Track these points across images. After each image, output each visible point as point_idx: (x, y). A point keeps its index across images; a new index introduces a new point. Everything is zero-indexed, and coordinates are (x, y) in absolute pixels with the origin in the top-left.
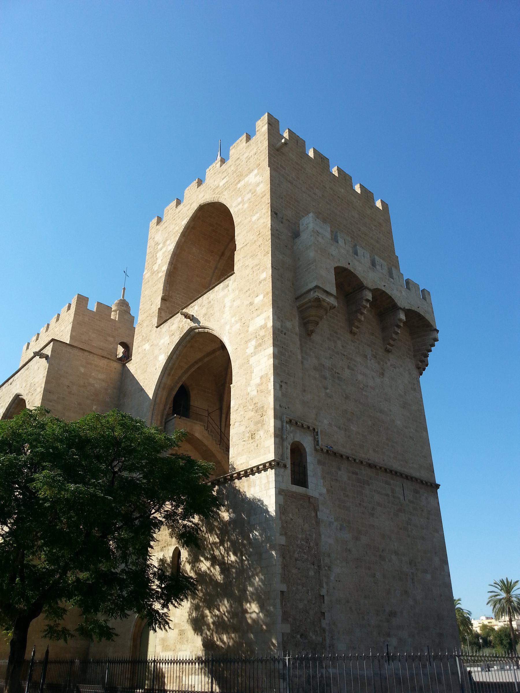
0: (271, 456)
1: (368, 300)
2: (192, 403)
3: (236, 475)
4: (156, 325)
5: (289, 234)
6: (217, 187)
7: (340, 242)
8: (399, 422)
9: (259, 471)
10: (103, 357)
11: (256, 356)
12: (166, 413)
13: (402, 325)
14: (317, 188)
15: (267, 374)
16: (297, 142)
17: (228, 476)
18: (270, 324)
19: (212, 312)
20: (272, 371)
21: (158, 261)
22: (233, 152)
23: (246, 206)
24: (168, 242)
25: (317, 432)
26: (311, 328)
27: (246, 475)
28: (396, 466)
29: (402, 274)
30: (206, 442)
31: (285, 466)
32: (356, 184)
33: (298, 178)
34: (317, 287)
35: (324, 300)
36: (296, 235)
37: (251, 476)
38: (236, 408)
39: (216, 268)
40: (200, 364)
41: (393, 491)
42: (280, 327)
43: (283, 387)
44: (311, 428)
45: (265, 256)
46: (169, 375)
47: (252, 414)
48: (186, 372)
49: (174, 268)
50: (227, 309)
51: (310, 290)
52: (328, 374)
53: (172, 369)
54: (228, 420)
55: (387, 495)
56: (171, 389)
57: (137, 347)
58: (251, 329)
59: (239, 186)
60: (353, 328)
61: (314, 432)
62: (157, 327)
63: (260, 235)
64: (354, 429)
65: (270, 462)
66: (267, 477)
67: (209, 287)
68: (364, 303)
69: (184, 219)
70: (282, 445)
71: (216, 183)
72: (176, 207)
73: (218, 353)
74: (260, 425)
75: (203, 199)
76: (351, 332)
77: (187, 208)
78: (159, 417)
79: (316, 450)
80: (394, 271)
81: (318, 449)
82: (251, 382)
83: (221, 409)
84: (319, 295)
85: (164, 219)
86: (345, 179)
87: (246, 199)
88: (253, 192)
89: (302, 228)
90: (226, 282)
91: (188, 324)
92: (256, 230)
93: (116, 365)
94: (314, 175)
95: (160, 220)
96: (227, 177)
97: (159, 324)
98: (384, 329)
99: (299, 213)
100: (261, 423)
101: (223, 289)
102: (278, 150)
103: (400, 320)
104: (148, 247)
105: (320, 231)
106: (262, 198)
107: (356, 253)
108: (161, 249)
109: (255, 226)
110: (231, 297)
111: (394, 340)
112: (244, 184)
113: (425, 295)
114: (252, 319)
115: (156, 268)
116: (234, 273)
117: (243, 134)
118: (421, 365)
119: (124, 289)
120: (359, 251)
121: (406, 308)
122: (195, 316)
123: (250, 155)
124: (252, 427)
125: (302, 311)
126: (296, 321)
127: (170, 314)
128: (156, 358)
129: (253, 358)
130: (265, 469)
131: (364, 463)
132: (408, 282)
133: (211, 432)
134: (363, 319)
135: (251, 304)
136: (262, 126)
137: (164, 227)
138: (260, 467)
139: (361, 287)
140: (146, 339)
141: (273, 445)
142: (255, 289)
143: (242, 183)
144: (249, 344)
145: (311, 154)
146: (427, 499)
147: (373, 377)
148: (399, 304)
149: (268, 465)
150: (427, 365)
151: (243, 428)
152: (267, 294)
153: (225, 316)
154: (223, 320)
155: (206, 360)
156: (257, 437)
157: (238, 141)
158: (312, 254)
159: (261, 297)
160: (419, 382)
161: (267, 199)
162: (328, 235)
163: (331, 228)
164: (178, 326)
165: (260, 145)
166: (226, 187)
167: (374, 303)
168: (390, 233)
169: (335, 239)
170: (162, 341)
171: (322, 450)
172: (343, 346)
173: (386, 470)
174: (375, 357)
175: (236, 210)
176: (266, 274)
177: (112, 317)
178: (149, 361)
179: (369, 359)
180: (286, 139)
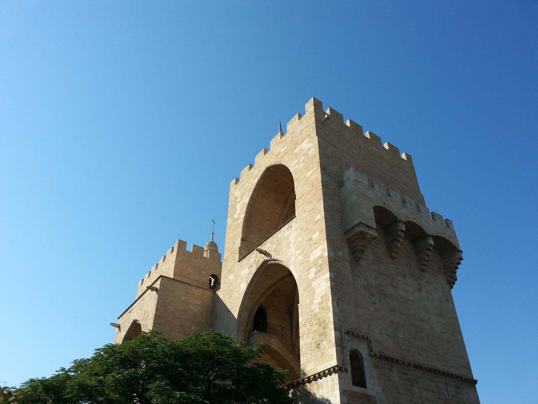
0: (334, 362)
1: (402, 231)
2: (268, 321)
3: (306, 379)
6: (279, 154)
8: (437, 329)
9: (325, 376)
10: (198, 287)
11: (317, 280)
12: (248, 329)
13: (432, 249)
16: (336, 116)
18: (326, 254)
20: (330, 292)
22: (290, 127)
23: (301, 166)
24: (244, 197)
26: (358, 255)
27: (315, 379)
28: (439, 366)
30: (281, 352)
31: (346, 370)
32: (385, 142)
35: (367, 233)
36: (341, 184)
38: (303, 323)
39: (282, 213)
40: (273, 289)
45: (318, 202)
46: (249, 298)
47: (317, 327)
48: (262, 296)
49: (250, 215)
50: (292, 245)
51: (355, 226)
53: (251, 293)
55: (434, 391)
58: (312, 259)
59: (295, 151)
61: (368, 340)
62: (239, 262)
65: (334, 368)
66: (332, 380)
67: (277, 228)
68: (400, 233)
70: (343, 353)
71: (278, 150)
73: (286, 279)
74: (323, 336)
78: (243, 333)
79: (371, 355)
80: (421, 207)
81: (373, 355)
83: (291, 324)
86: (376, 140)
88: (306, 155)
89: (345, 179)
91: (262, 258)
93: (209, 293)
95: (237, 181)
100: (324, 335)
101: (288, 229)
103: (430, 245)
105: (359, 180)
107: (389, 195)
109: (310, 180)
110: (294, 234)
111: (427, 261)
112: (299, 149)
113: (448, 223)
114: (312, 251)
118: (451, 280)
119: (213, 233)
121: (434, 235)
124: (317, 338)
125: (350, 242)
126: (346, 251)
128: (239, 285)
130: (330, 374)
131: (412, 365)
132: (433, 214)
134: (399, 246)
135: (310, 239)
136: (310, 107)
137: (241, 185)
139: (395, 220)
140: (231, 271)
142: (313, 228)
143: (297, 149)
145: (348, 124)
147: (412, 292)
149: (332, 369)
150: (456, 280)
151: (310, 340)
152: (322, 231)
153: (290, 250)
154: (289, 254)
155: (278, 285)
157: (293, 119)
158: (354, 198)
159: (317, 234)
161: (317, 159)
162: (366, 183)
163: (368, 177)
164: (255, 260)
165: (309, 120)
166: (286, 153)
168: (415, 177)
170: (243, 272)
171: (376, 355)
172: (385, 269)
173: (430, 370)
175: (294, 169)
176: (320, 216)
178: (234, 288)
180: (328, 115)
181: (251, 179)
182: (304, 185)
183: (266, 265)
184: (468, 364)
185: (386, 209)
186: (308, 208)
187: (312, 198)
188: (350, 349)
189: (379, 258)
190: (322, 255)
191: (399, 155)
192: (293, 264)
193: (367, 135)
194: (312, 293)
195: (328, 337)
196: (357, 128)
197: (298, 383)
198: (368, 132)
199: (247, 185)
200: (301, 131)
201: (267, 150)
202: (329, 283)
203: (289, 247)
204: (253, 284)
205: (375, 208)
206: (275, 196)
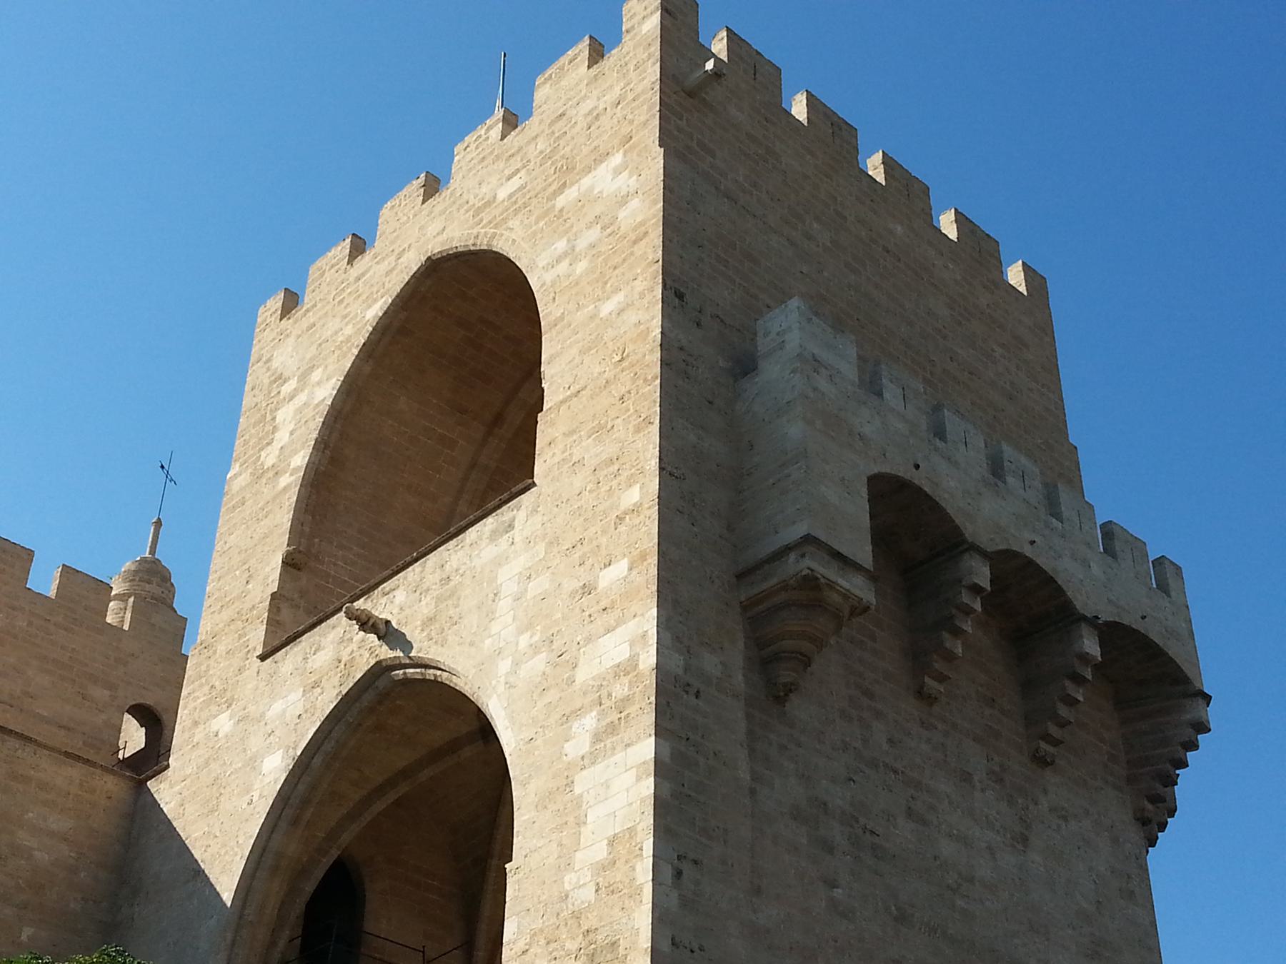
1: (976, 589)
2: (369, 925)
4: (259, 651)
6: (488, 204)
7: (886, 395)
10: (68, 755)
11: (599, 767)
18: (649, 659)
19: (451, 613)
22: (544, 93)
23: (581, 267)
24: (316, 375)
26: (785, 675)
29: (1091, 506)
34: (808, 539)
35: (831, 585)
36: (745, 366)
38: (521, 945)
39: (473, 466)
40: (404, 788)
42: (680, 672)
45: (638, 430)
46: (295, 822)
49: (332, 460)
50: (504, 604)
53: (305, 802)
57: (188, 723)
58: (584, 675)
62: (263, 658)
63: (625, 364)
67: (446, 526)
68: (966, 598)
69: (376, 301)
72: (350, 262)
73: (467, 752)
75: (440, 239)
76: (922, 694)
77: (384, 266)
80: (1064, 495)
84: (814, 565)
85: (308, 300)
86: (907, 191)
87: (582, 244)
88: (607, 223)
89: (763, 344)
90: (505, 514)
91: (367, 652)
93: (113, 786)
95: (291, 302)
96: (523, 173)
101: (494, 536)
102: (691, 94)
103: (1084, 658)
104: (247, 388)
106: (635, 242)
109: (611, 333)
110: (520, 563)
111: (1063, 724)
113: (1166, 575)
114: (589, 640)
115: (269, 457)
116: (534, 484)
118: (1154, 813)
119: (158, 524)
120: (948, 427)
121: (1104, 617)
122: (394, 624)
123: (601, 107)
126: (737, 653)
127: (309, 613)
128: (253, 763)
129: (585, 772)
132: (1109, 531)
134: (959, 650)
135: (587, 589)
137: (305, 323)
139: (953, 543)
140: (222, 699)
142: (603, 540)
143: (571, 193)
144: (576, 725)
148: (1078, 605)
150: (1172, 812)
152: (643, 557)
154: (488, 642)
157: (564, 60)
158: (795, 430)
159: (620, 568)
161: (652, 247)
162: (850, 371)
164: (336, 655)
165: (632, 75)
166: (518, 204)
167: (996, 599)
169: (872, 385)
170: (278, 706)
172: (890, 741)
174: (1000, 781)
175: (548, 277)
176: (641, 492)
177: (109, 620)
181: (350, 301)
182: (582, 352)
183: (381, 683)
185: (919, 490)
186: (591, 451)
187: (612, 413)
189: (869, 694)
190: (633, 662)
192: (501, 689)
194: (572, 818)
199: (333, 325)
200: (595, 117)
201: (437, 181)
203: (491, 616)
204: (317, 760)
205: (874, 481)
206: (450, 391)
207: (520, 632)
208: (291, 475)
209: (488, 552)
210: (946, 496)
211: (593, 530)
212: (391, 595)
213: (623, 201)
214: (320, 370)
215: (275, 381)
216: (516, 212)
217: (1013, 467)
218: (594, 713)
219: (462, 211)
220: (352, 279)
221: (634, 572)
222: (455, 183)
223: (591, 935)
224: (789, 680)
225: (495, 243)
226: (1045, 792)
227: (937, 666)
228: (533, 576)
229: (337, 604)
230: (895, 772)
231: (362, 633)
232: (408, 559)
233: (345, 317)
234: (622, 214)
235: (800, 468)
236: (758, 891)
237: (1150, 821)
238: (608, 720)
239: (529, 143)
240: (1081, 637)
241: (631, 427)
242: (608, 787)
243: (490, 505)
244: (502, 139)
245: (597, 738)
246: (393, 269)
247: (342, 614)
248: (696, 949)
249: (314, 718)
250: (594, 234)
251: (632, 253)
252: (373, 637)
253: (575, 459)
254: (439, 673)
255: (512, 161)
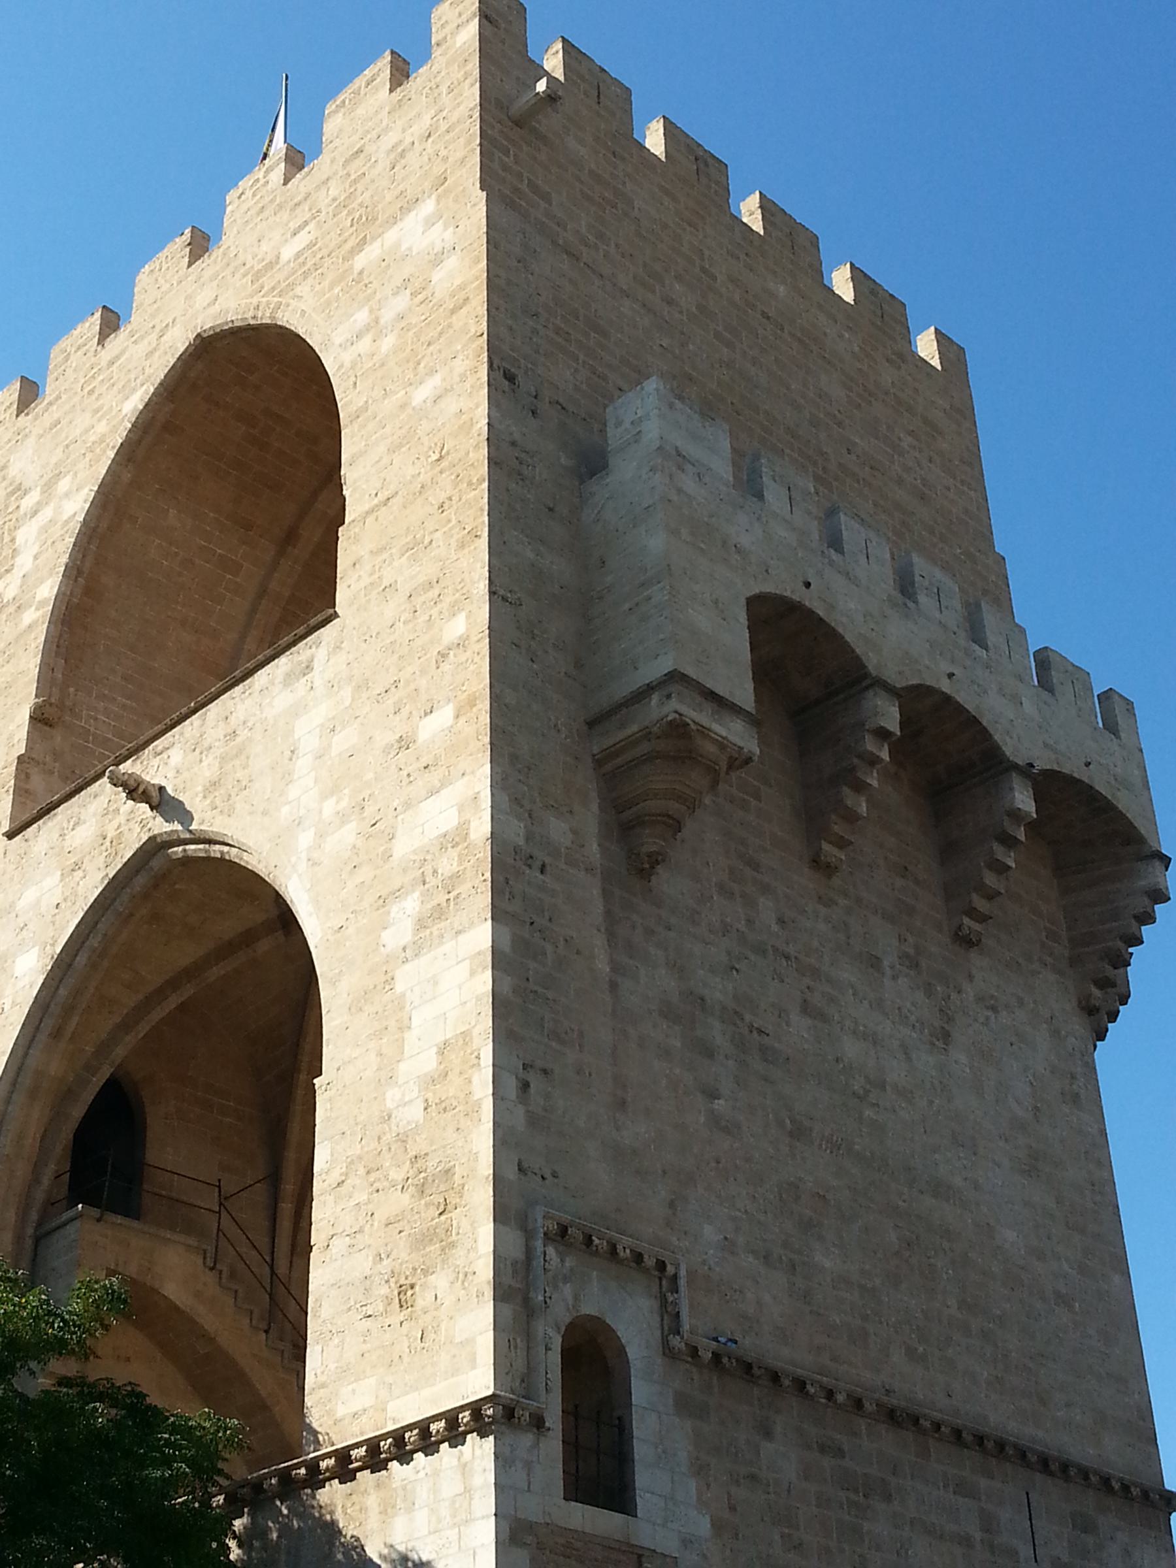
0: (478, 1381)
1: (883, 734)
2: (152, 1155)
4: (6, 827)
5: (563, 460)
6: (270, 265)
8: (1010, 1235)
9: (428, 1446)
11: (424, 960)
12: (40, 1195)
14: (678, 278)
15: (466, 1036)
16: (596, 92)
17: (297, 1466)
18: (481, 826)
19: (239, 775)
20: (487, 1022)
21: (19, 560)
23: (388, 343)
24: (64, 485)
25: (675, 1278)
26: (650, 842)
27: (376, 1459)
28: (1002, 1417)
29: (1022, 631)
30: (208, 1321)
31: (538, 1423)
33: (601, 236)
34: (675, 677)
35: (704, 732)
36: (592, 463)
37: (394, 1465)
38: (335, 1177)
39: (262, 592)
40: (188, 991)
41: (988, 1524)
42: (521, 842)
43: (532, 1090)
44: (649, 1262)
45: (462, 546)
46: (57, 1034)
47: (405, 1200)
48: (125, 1026)
49: (88, 591)
50: (303, 763)
51: (650, 688)
52: (717, 1033)
53: (68, 1010)
54: (304, 1224)
56: (67, 1095)
58: (403, 847)
60: (825, 846)
61: (662, 1276)
62: (10, 835)
63: (444, 464)
64: (828, 1264)
65: (476, 1408)
66: (464, 1469)
67: (230, 669)
68: (870, 744)
69: (134, 390)
70: (529, 1336)
72: (101, 342)
73: (264, 946)
74: (435, 1248)
77: (143, 348)
80: (990, 617)
82: (403, 1067)
83: (274, 1178)
84: (683, 709)
85: (50, 390)
87: (387, 316)
88: (420, 289)
89: (615, 436)
90: (302, 652)
91: (139, 825)
92: (425, 440)
94: (665, 226)
96: (311, 226)
97: (17, 823)
98: (948, 851)
99: (604, 378)
100: (439, 1239)
102: (518, 123)
103: (1016, 815)
106: (453, 312)
107: (835, 542)
108: (36, 513)
110: (320, 713)
112: (378, 257)
113: (1114, 713)
114: (408, 805)
116: (336, 615)
117: (378, 55)
121: (1040, 765)
122: (170, 790)
123: (408, 140)
124: (404, 1256)
126: (590, 817)
127: (65, 779)
129: (407, 966)
130: (455, 1436)
131: (869, 1407)
132: (1044, 660)
133: (233, 1275)
134: (863, 809)
135: (404, 743)
136: (457, 31)
137: (47, 419)
138: (434, 1427)
139: (852, 678)
141: (490, 1335)
142: (423, 683)
144: (394, 909)
145: (655, 141)
146: (1127, 1553)
148: (1008, 751)
149: (465, 1417)
150: (1124, 1000)
151: (363, 1263)
152: (472, 702)
153: (293, 792)
154: (285, 810)
155: (215, 972)
156: (423, 1299)
157: (360, 81)
158: (656, 542)
159: (444, 716)
160: (1091, 1069)
161: (474, 317)
164: (100, 831)
165: (446, 100)
166: (308, 266)
168: (972, 458)
170: (30, 895)
171: (694, 1351)
172: (781, 921)
173: (958, 1433)
174: (916, 965)
176: (468, 622)
179: (888, 971)
180: (552, 80)
182: (392, 450)
183: (156, 863)
184: (1145, 1413)
185: (811, 613)
187: (430, 525)
188: (568, 1320)
190: (462, 831)
191: (908, 340)
192: (303, 866)
193: (750, 213)
194: (394, 1022)
195: (460, 1252)
196: (698, 172)
197: (285, 1477)
198: (754, 200)
200: (400, 154)
201: (206, 238)
202: (484, 982)
203: (288, 778)
205: (754, 602)
206: (229, 500)
207: (324, 797)
208: (37, 609)
209: (282, 700)
210: (844, 620)
211: (410, 669)
212: (165, 755)
213: (437, 260)
214: (69, 478)
215: (13, 493)
216: (305, 275)
217: (926, 583)
218: (416, 895)
219: (238, 276)
220: (104, 363)
221: (462, 720)
222: (228, 240)
223: (420, 1163)
224: (654, 848)
225: (279, 315)
226: (971, 977)
227: (836, 828)
228: (338, 729)
229: (100, 767)
230: (787, 958)
231: (131, 802)
232: (184, 710)
233: (97, 411)
234: (437, 276)
235: (662, 589)
236: (622, 1104)
237: (1098, 1010)
238: (435, 902)
239: (318, 188)
240: (1012, 789)
241: (453, 542)
242: (436, 983)
243: (283, 642)
244: (285, 184)
245: (421, 924)
246: (155, 349)
247: (105, 779)
248: (548, 1175)
249: (76, 908)
250: (402, 302)
251: (450, 326)
252: (144, 807)
253: (386, 583)
254: (226, 849)
255: (298, 211)
